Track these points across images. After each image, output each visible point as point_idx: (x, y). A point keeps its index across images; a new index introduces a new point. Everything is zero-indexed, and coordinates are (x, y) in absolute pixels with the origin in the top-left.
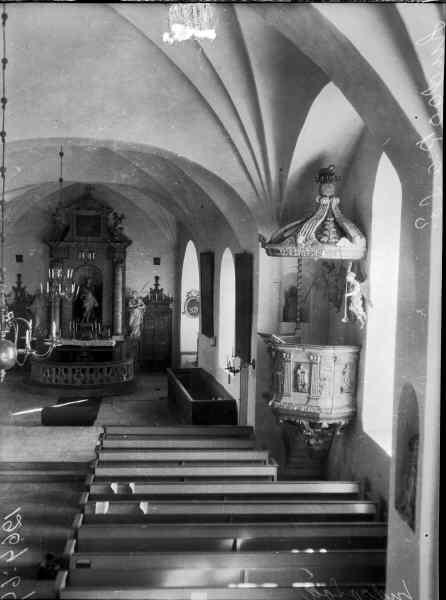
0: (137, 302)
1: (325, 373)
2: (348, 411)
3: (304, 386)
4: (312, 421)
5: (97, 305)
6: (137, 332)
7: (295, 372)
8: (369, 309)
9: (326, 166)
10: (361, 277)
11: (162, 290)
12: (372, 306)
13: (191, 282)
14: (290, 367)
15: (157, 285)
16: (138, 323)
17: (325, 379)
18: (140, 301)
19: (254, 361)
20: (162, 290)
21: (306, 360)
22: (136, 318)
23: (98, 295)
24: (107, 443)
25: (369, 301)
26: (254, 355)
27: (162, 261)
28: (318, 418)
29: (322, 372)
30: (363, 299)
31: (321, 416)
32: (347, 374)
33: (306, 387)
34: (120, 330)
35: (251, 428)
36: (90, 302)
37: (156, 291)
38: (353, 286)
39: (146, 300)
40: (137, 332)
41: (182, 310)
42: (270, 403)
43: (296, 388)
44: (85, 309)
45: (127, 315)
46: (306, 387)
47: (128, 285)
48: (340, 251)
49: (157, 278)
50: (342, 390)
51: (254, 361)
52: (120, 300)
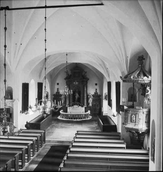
0: (90, 96)
2: (147, 128)
3: (133, 121)
4: (136, 131)
5: (79, 97)
6: (91, 105)
7: (131, 117)
9: (141, 55)
11: (98, 93)
13: (105, 91)
14: (130, 115)
15: (96, 91)
16: (91, 102)
18: (91, 96)
20: (98, 93)
22: (90, 101)
23: (80, 94)
24: (78, 136)
27: (98, 85)
28: (138, 131)
31: (139, 130)
33: (135, 121)
34: (86, 104)
35: (120, 133)
36: (77, 96)
37: (96, 93)
38: (148, 91)
39: (93, 95)
40: (91, 105)
41: (103, 98)
43: (131, 121)
44: (76, 98)
47: (88, 91)
48: (144, 80)
49: (96, 89)
50: (145, 122)
52: (86, 95)
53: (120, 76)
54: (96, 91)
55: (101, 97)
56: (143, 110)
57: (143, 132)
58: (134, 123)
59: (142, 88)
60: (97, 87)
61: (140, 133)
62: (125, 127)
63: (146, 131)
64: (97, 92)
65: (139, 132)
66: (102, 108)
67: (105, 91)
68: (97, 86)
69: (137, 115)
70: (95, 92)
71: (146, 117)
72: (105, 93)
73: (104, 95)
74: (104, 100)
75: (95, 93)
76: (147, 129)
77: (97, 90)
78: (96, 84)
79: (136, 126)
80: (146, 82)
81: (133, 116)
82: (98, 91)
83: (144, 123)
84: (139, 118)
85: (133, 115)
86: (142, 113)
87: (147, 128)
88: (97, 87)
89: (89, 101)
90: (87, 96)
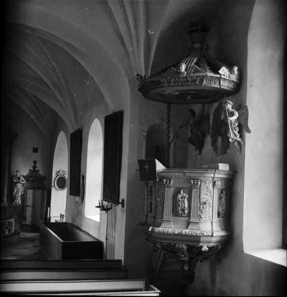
0: (19, 178)
1: (204, 197)
2: (223, 233)
3: (183, 210)
7: (175, 197)
8: (247, 135)
10: (241, 107)
11: (38, 171)
12: (249, 131)
14: (169, 193)
17: (205, 203)
18: (22, 178)
19: (123, 200)
20: (38, 171)
21: (186, 185)
22: (18, 191)
25: (247, 127)
26: (123, 195)
27: (39, 151)
28: (199, 242)
29: (202, 196)
30: (240, 126)
31: (202, 239)
32: (223, 200)
33: (186, 212)
35: (120, 261)
37: (34, 171)
39: (26, 177)
41: (53, 185)
42: (150, 229)
43: (175, 213)
45: (12, 186)
46: (186, 212)
49: (35, 162)
50: (219, 214)
51: (123, 200)
53: (138, 75)
54: (35, 167)
55: (46, 182)
56: (216, 176)
57: (211, 245)
58: (187, 218)
59: (191, 122)
60: (37, 157)
61: (205, 248)
62: (153, 231)
63: (218, 242)
64: (37, 169)
65: (201, 247)
66: (49, 208)
67: (61, 165)
68: (38, 154)
69: (194, 191)
70: (32, 169)
71: (220, 198)
72: (59, 172)
73: (54, 176)
74: (53, 190)
75: (30, 170)
76: (223, 236)
77: (37, 165)
78: (35, 150)
79: (191, 226)
80: (225, 85)
81: (180, 196)
82: (39, 167)
83: (216, 219)
84: (203, 201)
85: (182, 192)
86: (211, 185)
87: (223, 233)
88: (37, 157)
89: (15, 190)
90: (11, 178)
